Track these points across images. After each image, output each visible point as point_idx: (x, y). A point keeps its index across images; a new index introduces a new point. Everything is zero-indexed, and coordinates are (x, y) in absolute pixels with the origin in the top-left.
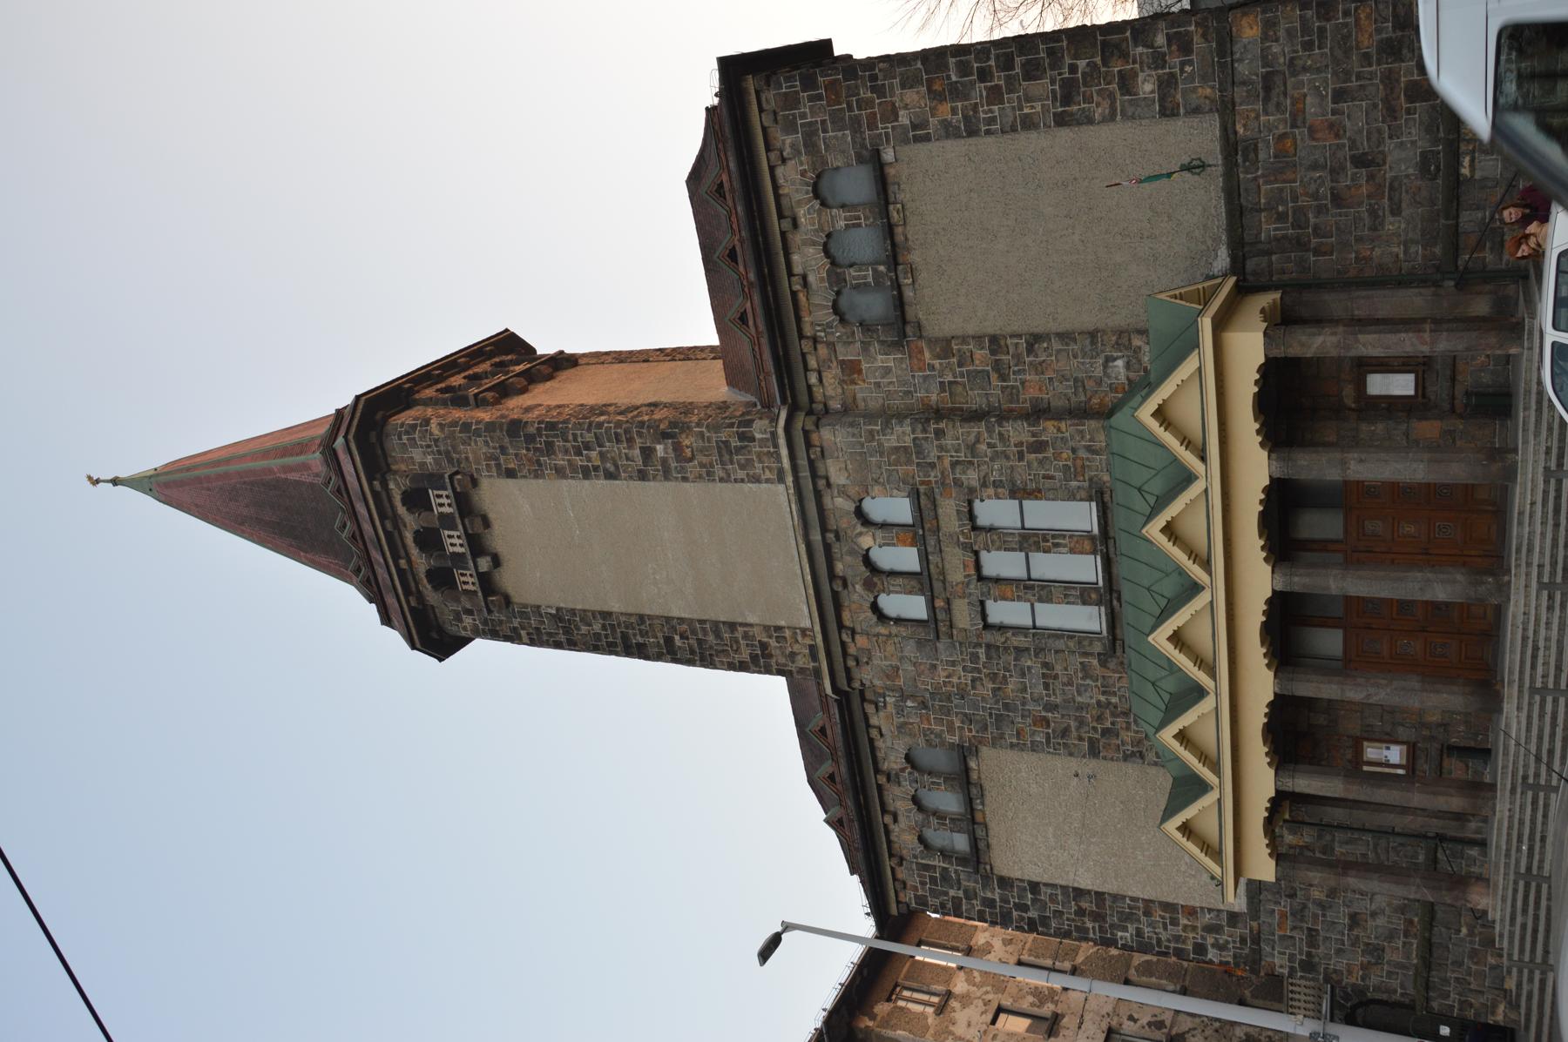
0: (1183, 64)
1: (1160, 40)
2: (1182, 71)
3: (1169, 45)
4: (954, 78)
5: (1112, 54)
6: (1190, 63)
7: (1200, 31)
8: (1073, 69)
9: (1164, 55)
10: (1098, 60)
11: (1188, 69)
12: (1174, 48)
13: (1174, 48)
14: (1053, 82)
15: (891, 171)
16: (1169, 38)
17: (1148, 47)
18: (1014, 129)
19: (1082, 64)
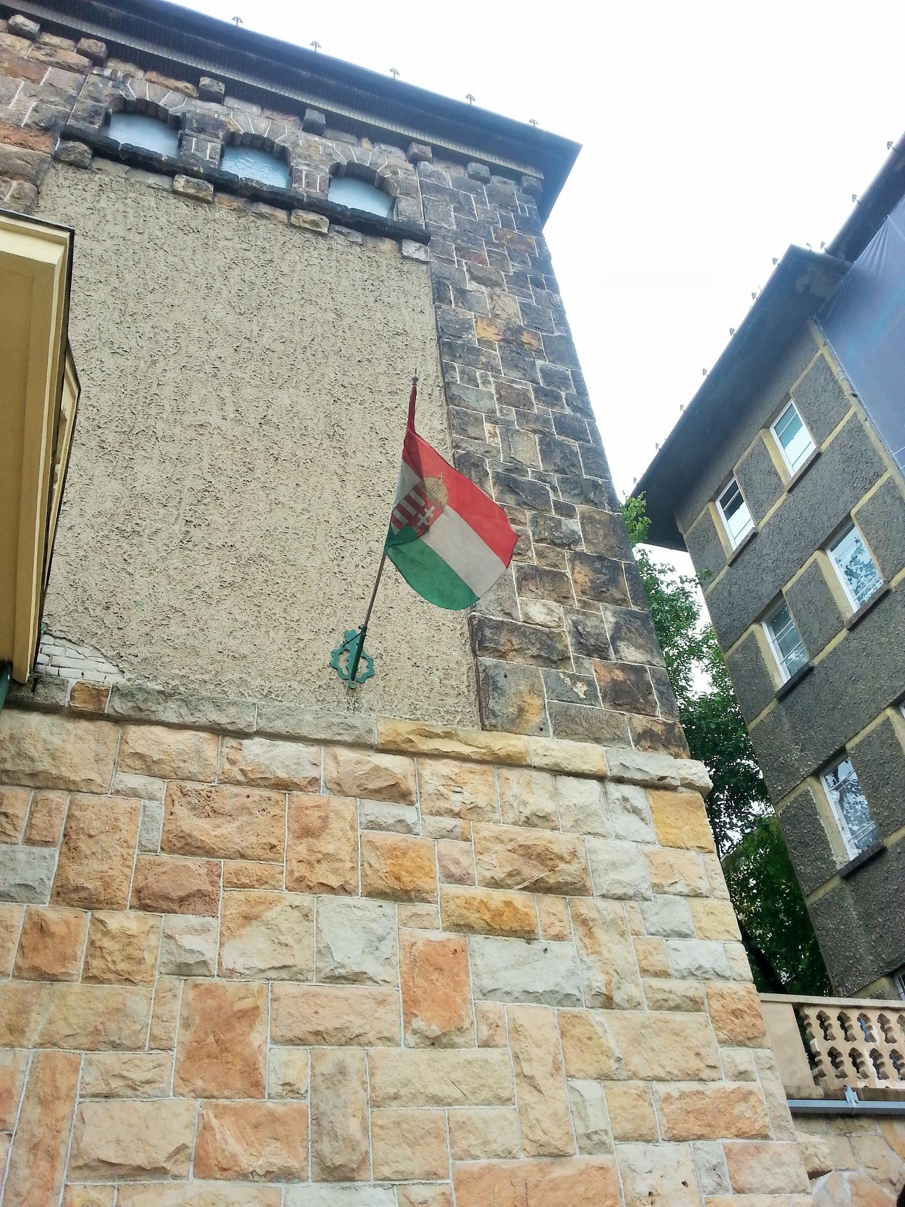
0: (590, 683)
1: (632, 655)
2: (575, 679)
3: (624, 668)
4: (539, 363)
5: (597, 571)
6: (591, 696)
7: (658, 729)
8: (567, 511)
9: (604, 657)
10: (583, 548)
11: (581, 689)
12: (619, 675)
13: (619, 675)
14: (541, 477)
15: (387, 245)
16: (638, 670)
17: (617, 628)
18: (450, 399)
19: (574, 525)
